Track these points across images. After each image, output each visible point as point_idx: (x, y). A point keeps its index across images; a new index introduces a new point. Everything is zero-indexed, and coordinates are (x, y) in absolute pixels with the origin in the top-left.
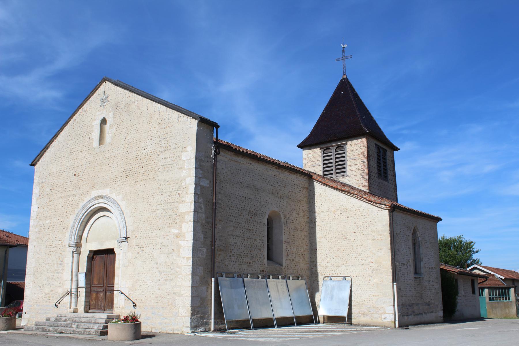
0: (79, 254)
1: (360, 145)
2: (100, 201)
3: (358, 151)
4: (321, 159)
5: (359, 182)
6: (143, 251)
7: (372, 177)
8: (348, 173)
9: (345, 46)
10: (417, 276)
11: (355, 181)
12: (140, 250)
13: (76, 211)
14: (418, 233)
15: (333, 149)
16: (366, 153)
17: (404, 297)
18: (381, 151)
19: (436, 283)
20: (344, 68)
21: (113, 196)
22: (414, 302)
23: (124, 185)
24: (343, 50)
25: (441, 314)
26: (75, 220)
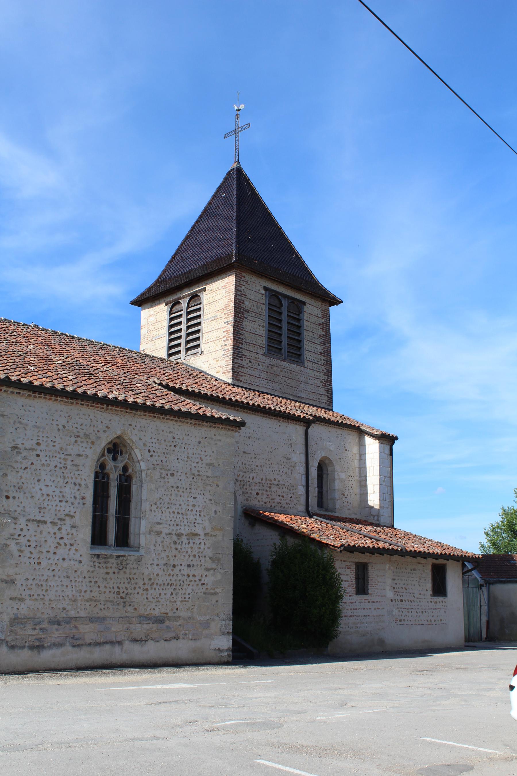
1: (224, 290)
3: (220, 302)
4: (166, 324)
5: (219, 364)
7: (245, 353)
8: (204, 347)
9: (242, 107)
10: (97, 552)
11: (212, 362)
14: (137, 451)
15: (184, 303)
16: (232, 304)
17: (28, 602)
18: (285, 303)
19: (207, 570)
20: (237, 148)
22: (83, 614)
24: (238, 116)
25: (225, 643)
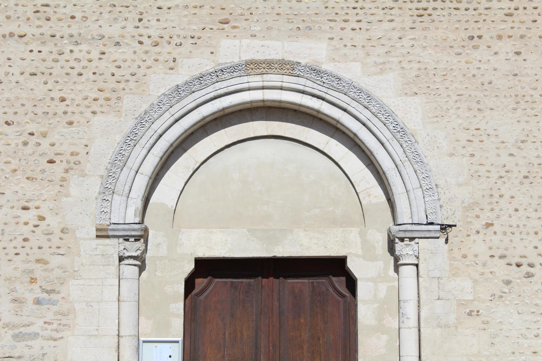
0: (142, 268)
2: (274, 79)
6: (529, 275)
12: (514, 273)
13: (134, 104)
21: (351, 71)
23: (405, 42)
26: (131, 139)
